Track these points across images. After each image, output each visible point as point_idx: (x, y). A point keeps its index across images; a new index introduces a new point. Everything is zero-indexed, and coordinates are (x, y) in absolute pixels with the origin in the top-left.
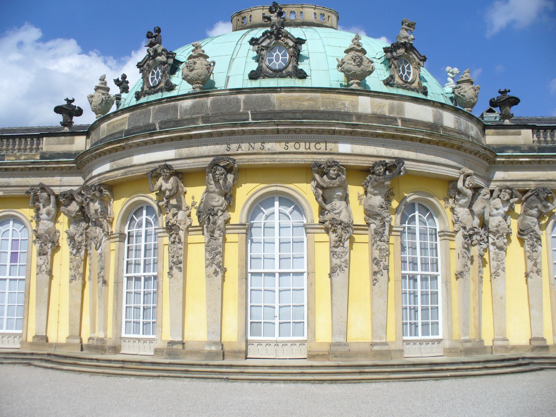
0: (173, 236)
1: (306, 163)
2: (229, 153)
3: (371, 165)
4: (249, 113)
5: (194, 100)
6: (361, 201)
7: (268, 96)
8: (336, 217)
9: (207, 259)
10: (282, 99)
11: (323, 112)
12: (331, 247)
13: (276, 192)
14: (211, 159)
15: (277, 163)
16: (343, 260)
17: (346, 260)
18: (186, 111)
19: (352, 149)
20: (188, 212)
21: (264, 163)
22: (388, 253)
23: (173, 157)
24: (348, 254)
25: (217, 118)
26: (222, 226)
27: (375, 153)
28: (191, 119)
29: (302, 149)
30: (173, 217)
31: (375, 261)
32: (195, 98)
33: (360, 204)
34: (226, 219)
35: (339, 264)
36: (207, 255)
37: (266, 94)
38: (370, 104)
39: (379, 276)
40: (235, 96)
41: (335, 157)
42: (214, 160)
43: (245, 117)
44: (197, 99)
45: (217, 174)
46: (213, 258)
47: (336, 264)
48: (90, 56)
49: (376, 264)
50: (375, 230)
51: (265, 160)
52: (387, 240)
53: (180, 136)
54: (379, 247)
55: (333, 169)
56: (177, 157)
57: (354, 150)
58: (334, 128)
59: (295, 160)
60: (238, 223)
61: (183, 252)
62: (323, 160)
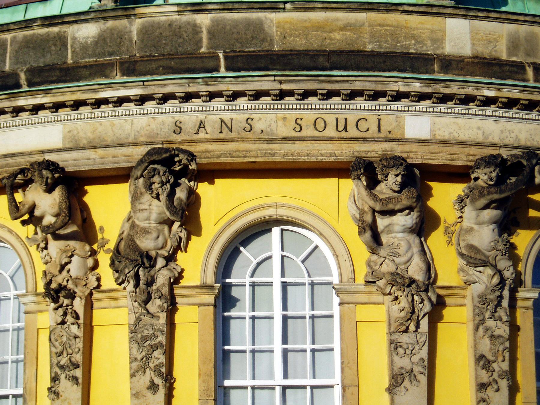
0: (61, 311)
1: (339, 159)
2: (178, 138)
3: (472, 164)
4: (221, 55)
9: (133, 360)
11: (373, 54)
12: (391, 334)
14: (141, 151)
15: (278, 159)
16: (415, 359)
18: (85, 48)
19: (432, 131)
21: (253, 160)
23: (60, 145)
25: (154, 65)
26: (165, 290)
27: (480, 138)
28: (97, 65)
29: (331, 132)
30: (61, 271)
31: (482, 361)
33: (449, 243)
35: (409, 368)
36: (135, 351)
38: (468, 36)
41: (398, 149)
42: (149, 153)
43: (211, 64)
46: (147, 358)
47: (402, 368)
48: (417, 218)
51: (252, 152)
54: (489, 333)
56: (67, 146)
57: (437, 132)
58: (396, 88)
60: (198, 283)
61: (81, 345)
62: (373, 154)
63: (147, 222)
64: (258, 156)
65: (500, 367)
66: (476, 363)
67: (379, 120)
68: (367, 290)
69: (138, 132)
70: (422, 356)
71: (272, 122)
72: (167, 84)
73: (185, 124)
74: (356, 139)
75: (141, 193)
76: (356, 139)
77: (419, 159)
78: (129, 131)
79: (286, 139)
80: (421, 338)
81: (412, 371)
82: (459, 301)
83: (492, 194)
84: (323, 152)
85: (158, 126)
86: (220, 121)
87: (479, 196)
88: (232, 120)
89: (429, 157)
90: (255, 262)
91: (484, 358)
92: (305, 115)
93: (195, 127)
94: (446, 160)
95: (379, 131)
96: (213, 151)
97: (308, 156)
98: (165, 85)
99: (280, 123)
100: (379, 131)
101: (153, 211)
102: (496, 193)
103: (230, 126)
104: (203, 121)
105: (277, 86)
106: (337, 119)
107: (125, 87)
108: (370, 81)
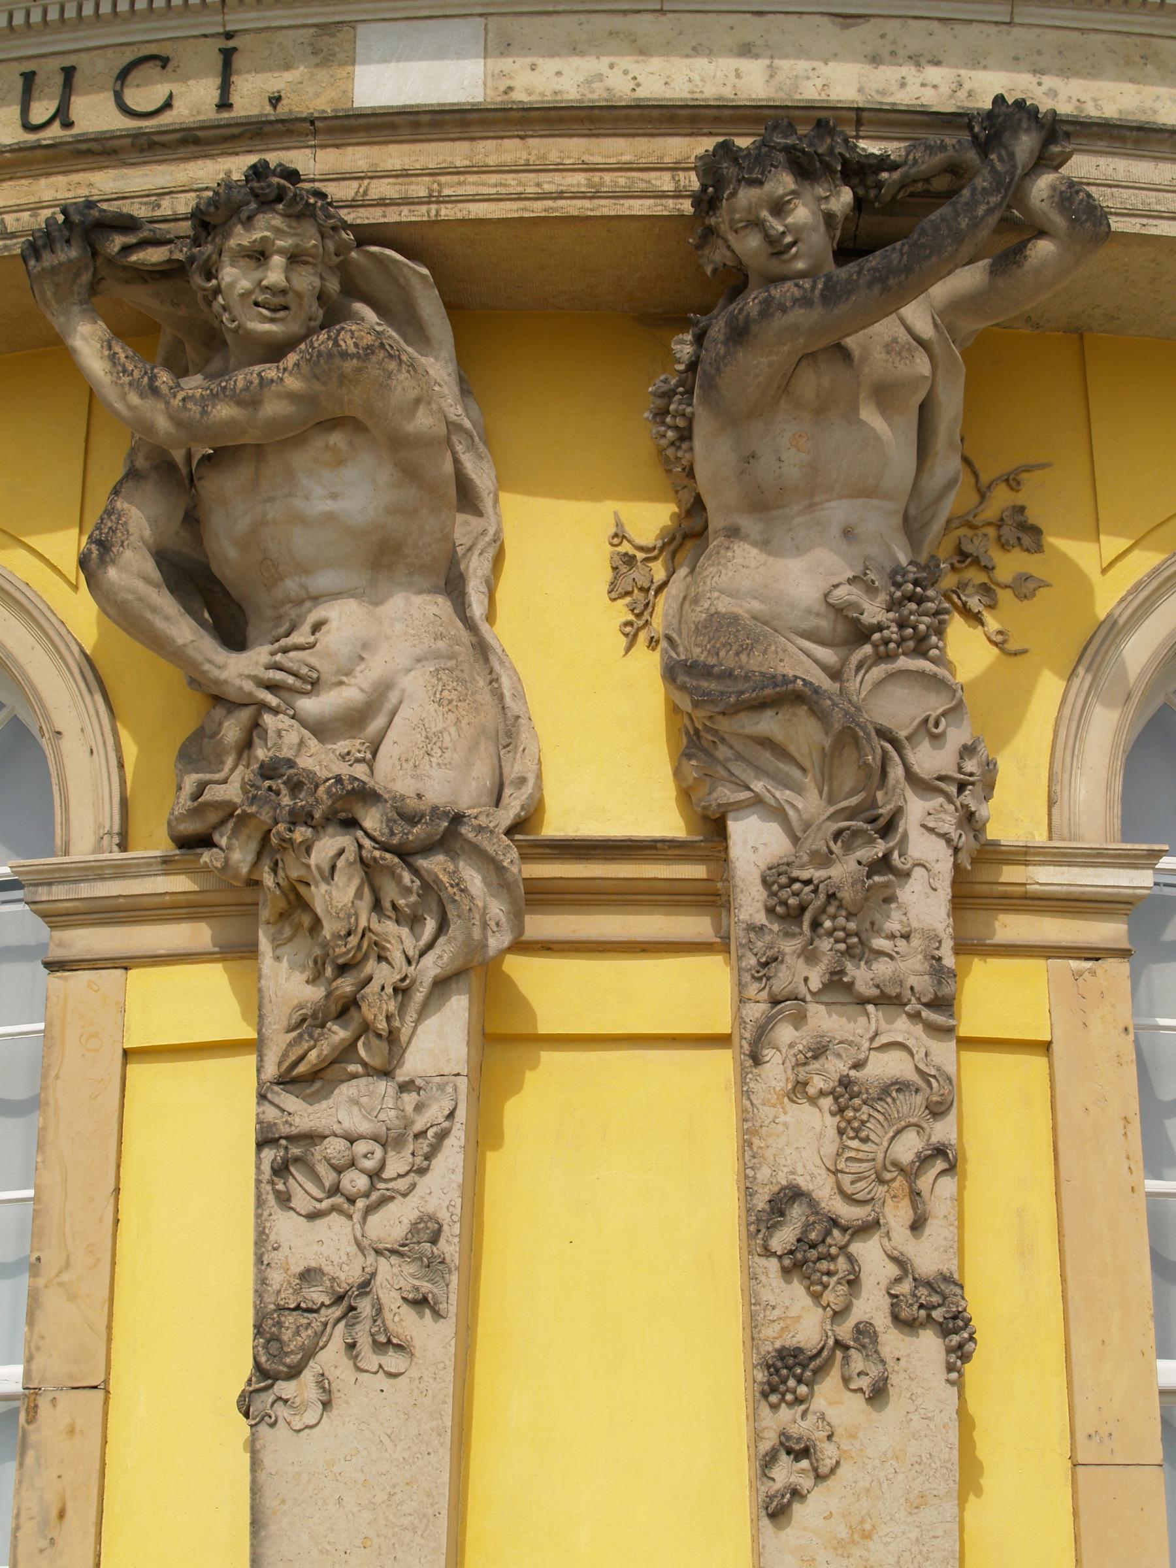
6: (642, 612)
8: (322, 761)
16: (391, 1223)
17: (428, 1230)
22: (942, 1131)
24: (451, 1157)
35: (350, 1274)
39: (834, 1402)
47: (308, 1275)
49: (801, 1263)
50: (776, 879)
52: (923, 983)
54: (835, 1066)
55: (241, 238)
65: (899, 1261)
66: (751, 1236)
68: (180, 884)
70: (430, 1208)
74: (101, 151)
76: (101, 151)
77: (419, 202)
80: (419, 1108)
81: (365, 1287)
82: (696, 926)
83: (783, 309)
87: (725, 343)
89: (470, 190)
91: (797, 1212)
94: (560, 195)
95: (224, 104)
100: (224, 104)
102: (805, 301)
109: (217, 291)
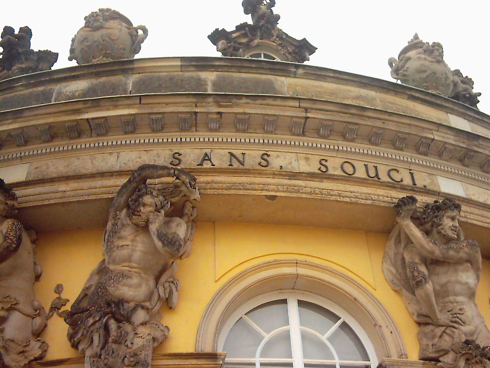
1: (377, 203)
5: (94, 81)
7: (269, 80)
10: (298, 88)
13: (293, 283)
15: (304, 196)
20: (38, 321)
21: (273, 193)
32: (98, 75)
34: (158, 334)
37: (264, 77)
40: (195, 74)
44: (103, 79)
45: (144, 205)
53: (50, 126)
55: (450, 213)
59: (349, 194)
63: (127, 264)
64: (278, 191)
67: (412, 174)
69: (125, 163)
71: (293, 161)
72: (170, 103)
73: (185, 156)
75: (123, 225)
78: (114, 163)
79: (311, 176)
84: (356, 194)
85: (152, 158)
86: (229, 155)
88: (244, 154)
90: (267, 337)
92: (330, 158)
93: (198, 159)
96: (221, 183)
97: (339, 196)
98: (167, 104)
99: (302, 162)
101: (137, 248)
103: (241, 159)
104: (209, 154)
105: (303, 115)
106: (366, 166)
107: (116, 107)
108: (404, 124)
109: (441, 224)
